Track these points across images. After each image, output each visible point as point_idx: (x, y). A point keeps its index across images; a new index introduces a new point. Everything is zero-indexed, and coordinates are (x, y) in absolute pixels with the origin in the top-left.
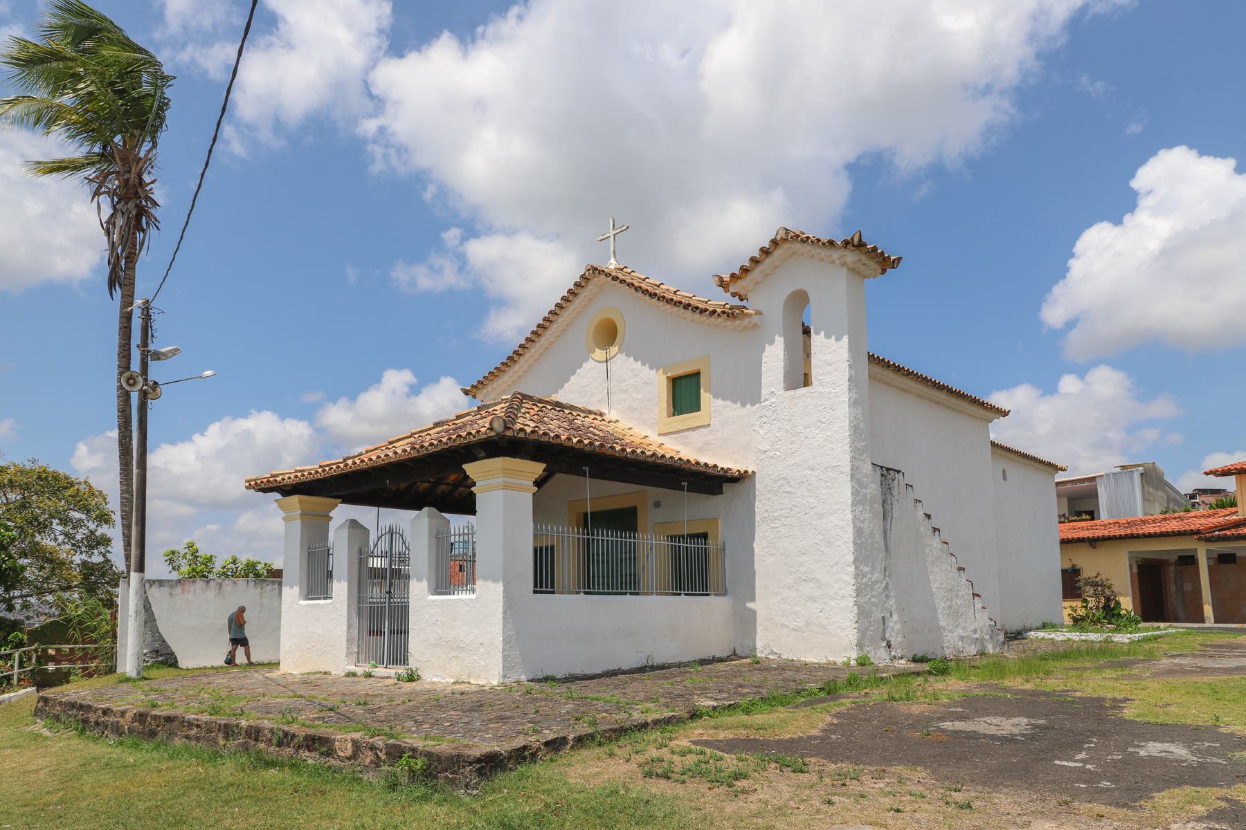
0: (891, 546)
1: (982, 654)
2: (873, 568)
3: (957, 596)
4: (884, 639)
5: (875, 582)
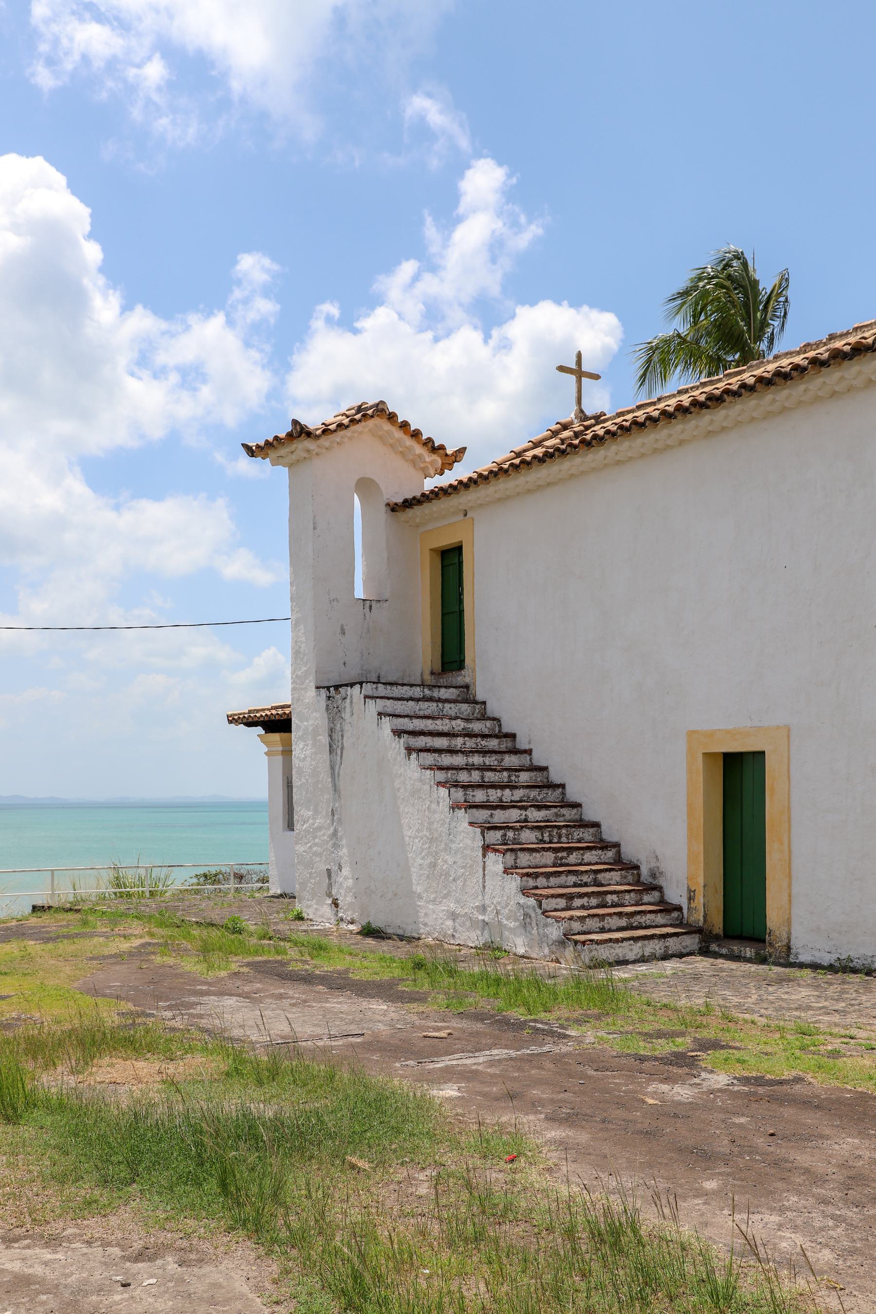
0: (341, 784)
1: (492, 950)
2: (316, 812)
3: (448, 849)
4: (329, 895)
5: (319, 828)
